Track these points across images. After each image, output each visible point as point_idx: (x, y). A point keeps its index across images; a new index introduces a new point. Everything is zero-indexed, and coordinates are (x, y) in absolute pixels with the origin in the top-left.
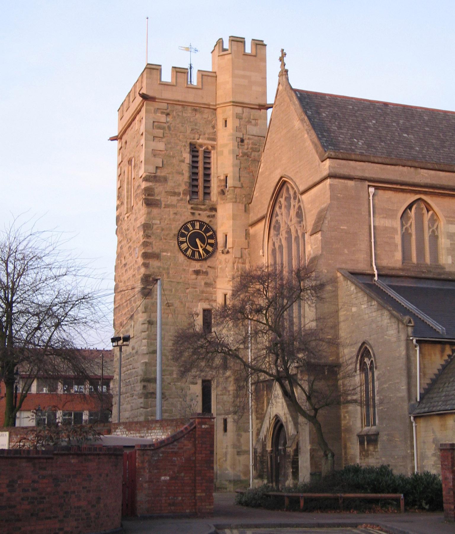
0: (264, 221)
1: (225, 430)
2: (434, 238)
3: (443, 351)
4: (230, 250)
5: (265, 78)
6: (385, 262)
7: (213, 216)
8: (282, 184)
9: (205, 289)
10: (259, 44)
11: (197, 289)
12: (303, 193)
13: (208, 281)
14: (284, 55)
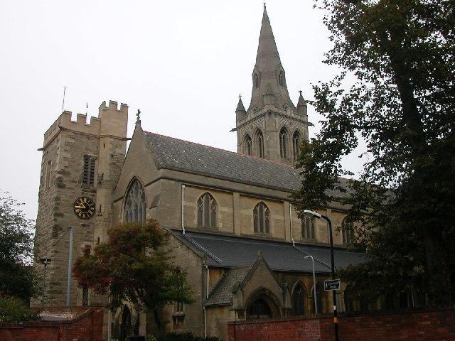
2: (214, 213)
3: (220, 273)
6: (188, 225)
8: (134, 181)
10: (125, 106)
12: (146, 186)
14: (139, 112)
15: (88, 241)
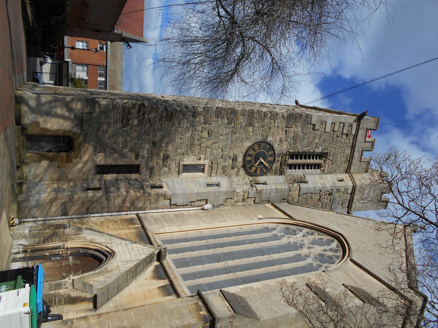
7: (276, 174)
9: (220, 167)
13: (227, 169)
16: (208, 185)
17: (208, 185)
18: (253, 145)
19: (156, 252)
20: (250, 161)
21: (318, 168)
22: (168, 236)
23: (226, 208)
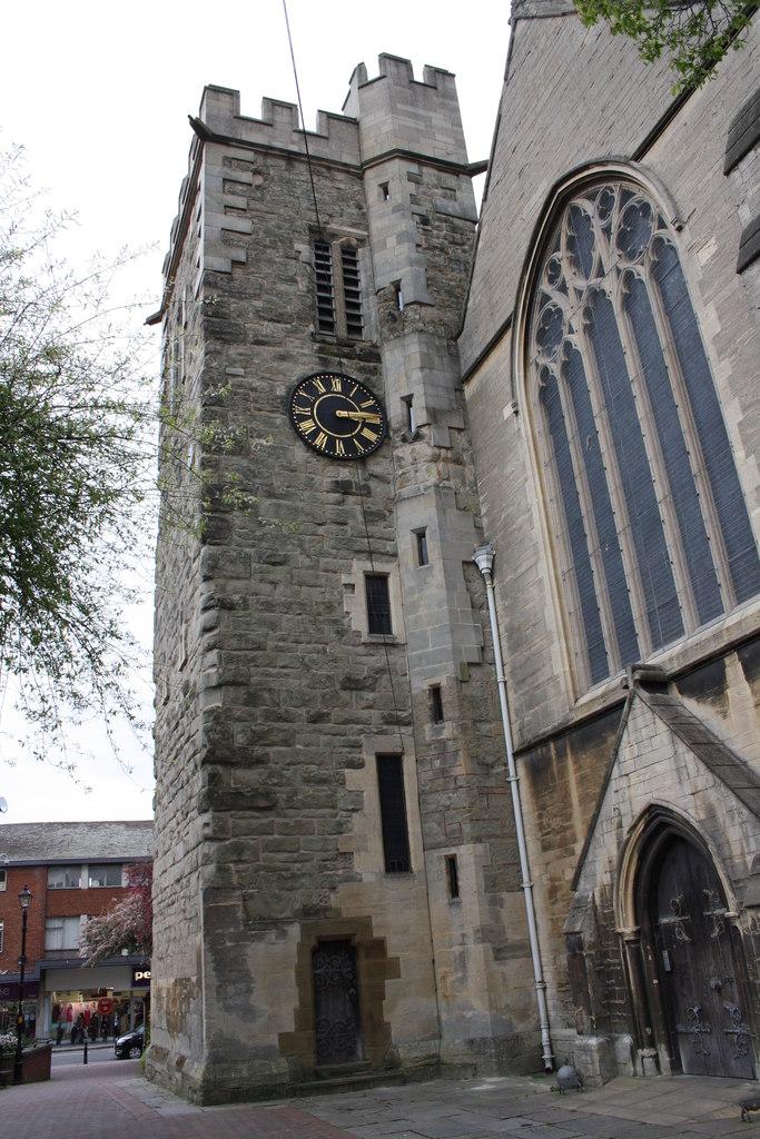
0: (510, 332)
1: (454, 890)
4: (425, 431)
5: (457, 124)
7: (375, 371)
11: (345, 527)
15: (370, 554)
16: (422, 560)
17: (422, 560)
18: (300, 435)
19: (644, 694)
20: (348, 444)
21: (354, 254)
22: (581, 665)
23: (483, 511)
